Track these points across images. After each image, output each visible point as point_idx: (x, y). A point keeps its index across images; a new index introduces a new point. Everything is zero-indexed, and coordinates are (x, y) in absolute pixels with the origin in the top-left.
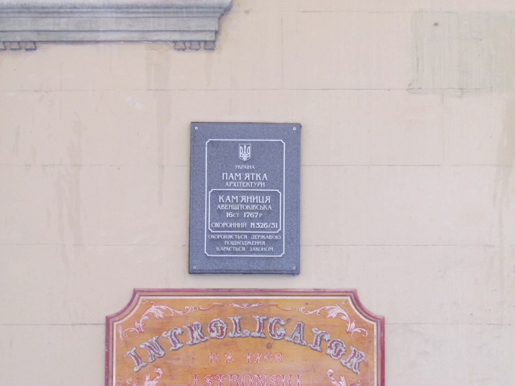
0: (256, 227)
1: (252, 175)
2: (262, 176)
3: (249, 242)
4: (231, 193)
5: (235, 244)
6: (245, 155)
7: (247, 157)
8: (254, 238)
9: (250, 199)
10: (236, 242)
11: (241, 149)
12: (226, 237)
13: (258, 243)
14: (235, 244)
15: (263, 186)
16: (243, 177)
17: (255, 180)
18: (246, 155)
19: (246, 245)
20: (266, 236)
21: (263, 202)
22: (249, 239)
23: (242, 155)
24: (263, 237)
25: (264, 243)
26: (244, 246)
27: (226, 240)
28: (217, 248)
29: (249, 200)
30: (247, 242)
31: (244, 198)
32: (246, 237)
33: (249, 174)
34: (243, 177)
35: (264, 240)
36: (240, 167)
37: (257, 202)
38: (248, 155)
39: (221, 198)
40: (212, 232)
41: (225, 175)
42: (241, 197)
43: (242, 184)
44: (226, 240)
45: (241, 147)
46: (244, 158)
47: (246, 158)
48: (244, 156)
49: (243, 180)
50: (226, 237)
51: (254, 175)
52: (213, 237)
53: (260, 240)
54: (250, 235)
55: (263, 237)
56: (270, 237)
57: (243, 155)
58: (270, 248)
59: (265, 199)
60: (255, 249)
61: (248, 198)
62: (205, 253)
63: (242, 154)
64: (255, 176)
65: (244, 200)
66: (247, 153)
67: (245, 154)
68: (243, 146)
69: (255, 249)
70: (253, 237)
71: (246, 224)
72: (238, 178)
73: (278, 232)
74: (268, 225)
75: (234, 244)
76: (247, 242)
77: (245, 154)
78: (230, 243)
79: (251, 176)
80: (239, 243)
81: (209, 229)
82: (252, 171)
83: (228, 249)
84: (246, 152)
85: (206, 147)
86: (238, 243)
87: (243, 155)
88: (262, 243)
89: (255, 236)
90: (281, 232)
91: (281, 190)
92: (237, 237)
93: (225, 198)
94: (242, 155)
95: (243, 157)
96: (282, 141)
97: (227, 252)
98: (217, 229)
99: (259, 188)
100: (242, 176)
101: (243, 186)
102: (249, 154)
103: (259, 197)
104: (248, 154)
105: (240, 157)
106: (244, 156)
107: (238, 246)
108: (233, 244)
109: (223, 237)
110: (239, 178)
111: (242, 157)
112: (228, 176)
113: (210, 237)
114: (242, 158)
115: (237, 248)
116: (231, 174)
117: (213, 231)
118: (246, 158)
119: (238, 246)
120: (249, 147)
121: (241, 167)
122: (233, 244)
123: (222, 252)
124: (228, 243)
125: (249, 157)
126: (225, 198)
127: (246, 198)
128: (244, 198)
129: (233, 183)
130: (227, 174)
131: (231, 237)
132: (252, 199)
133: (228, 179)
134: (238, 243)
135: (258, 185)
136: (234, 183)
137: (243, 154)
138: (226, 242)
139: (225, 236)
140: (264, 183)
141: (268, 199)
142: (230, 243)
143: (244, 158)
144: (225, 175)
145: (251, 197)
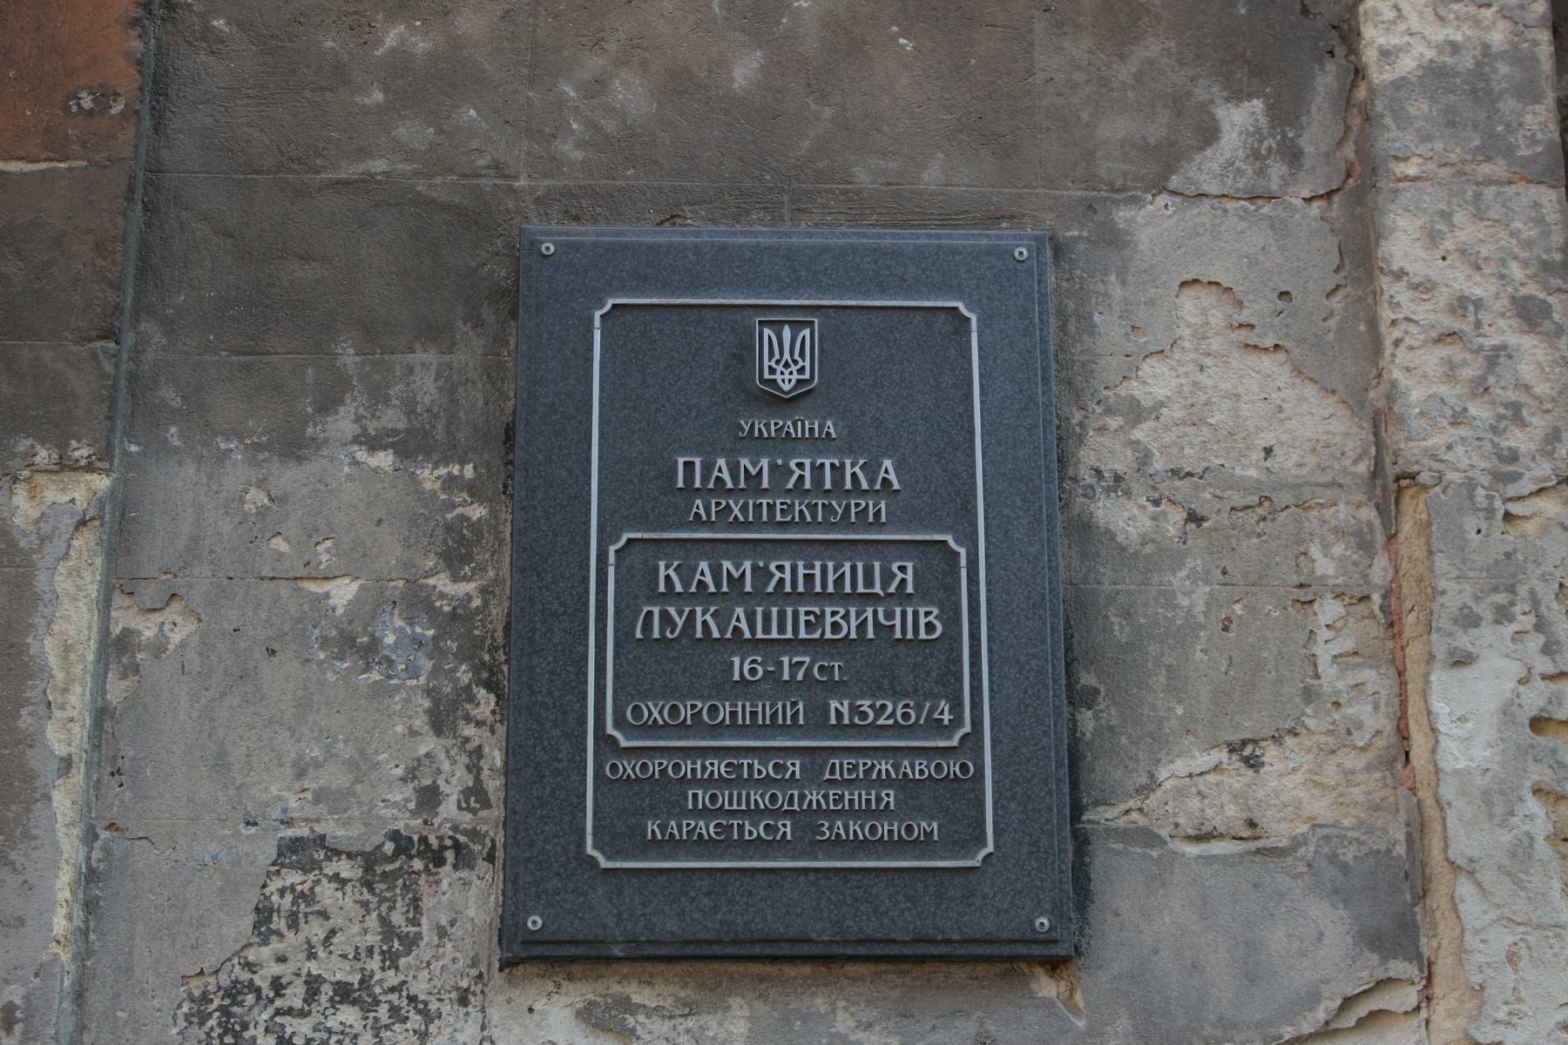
0: (856, 721)
1: (822, 465)
2: (871, 469)
3: (814, 796)
6: (787, 372)
7: (795, 377)
8: (838, 776)
9: (813, 575)
10: (748, 796)
12: (694, 770)
13: (859, 796)
14: (739, 804)
15: (877, 514)
16: (780, 472)
18: (794, 368)
20: (896, 767)
21: (877, 589)
22: (812, 776)
24: (884, 766)
25: (890, 797)
26: (790, 814)
27: (694, 782)
28: (652, 826)
29: (809, 578)
30: (802, 797)
31: (780, 568)
32: (795, 767)
33: (807, 462)
34: (780, 472)
35: (888, 782)
36: (764, 425)
37: (848, 589)
38: (801, 371)
41: (689, 466)
42: (766, 567)
43: (771, 507)
44: (694, 782)
45: (767, 332)
47: (790, 381)
48: (782, 373)
49: (777, 488)
50: (694, 770)
51: (832, 465)
52: (628, 768)
53: (868, 782)
56: (917, 769)
58: (923, 824)
61: (801, 571)
63: (774, 365)
64: (838, 470)
65: (781, 580)
66: (795, 362)
68: (777, 326)
70: (832, 772)
71: (800, 706)
74: (919, 708)
75: (735, 807)
76: (802, 797)
77: (787, 365)
78: (713, 798)
79: (818, 470)
80: (762, 796)
81: (610, 730)
82: (821, 443)
85: (597, 335)
86: (759, 798)
87: (780, 368)
88: (879, 800)
92: (750, 766)
93: (686, 573)
94: (772, 371)
95: (778, 377)
96: (960, 306)
97: (702, 846)
99: (850, 526)
100: (773, 467)
101: (779, 518)
102: (807, 364)
103: (860, 566)
104: (799, 366)
105: (763, 381)
106: (782, 373)
107: (754, 814)
108: (731, 803)
109: (677, 767)
110: (760, 482)
112: (708, 468)
113: (614, 768)
114: (775, 380)
115: (750, 825)
116: (721, 462)
117: (627, 738)
118: (793, 382)
119: (754, 814)
120: (807, 332)
121: (767, 426)
122: (731, 803)
123: (671, 846)
125: (807, 376)
127: (794, 569)
130: (697, 461)
131: (718, 767)
132: (828, 573)
133: (705, 478)
134: (759, 798)
135: (853, 510)
136: (731, 502)
137: (778, 362)
138: (694, 796)
139: (689, 766)
140: (883, 505)
141: (907, 573)
142: (713, 798)
144: (689, 466)
145: (818, 564)
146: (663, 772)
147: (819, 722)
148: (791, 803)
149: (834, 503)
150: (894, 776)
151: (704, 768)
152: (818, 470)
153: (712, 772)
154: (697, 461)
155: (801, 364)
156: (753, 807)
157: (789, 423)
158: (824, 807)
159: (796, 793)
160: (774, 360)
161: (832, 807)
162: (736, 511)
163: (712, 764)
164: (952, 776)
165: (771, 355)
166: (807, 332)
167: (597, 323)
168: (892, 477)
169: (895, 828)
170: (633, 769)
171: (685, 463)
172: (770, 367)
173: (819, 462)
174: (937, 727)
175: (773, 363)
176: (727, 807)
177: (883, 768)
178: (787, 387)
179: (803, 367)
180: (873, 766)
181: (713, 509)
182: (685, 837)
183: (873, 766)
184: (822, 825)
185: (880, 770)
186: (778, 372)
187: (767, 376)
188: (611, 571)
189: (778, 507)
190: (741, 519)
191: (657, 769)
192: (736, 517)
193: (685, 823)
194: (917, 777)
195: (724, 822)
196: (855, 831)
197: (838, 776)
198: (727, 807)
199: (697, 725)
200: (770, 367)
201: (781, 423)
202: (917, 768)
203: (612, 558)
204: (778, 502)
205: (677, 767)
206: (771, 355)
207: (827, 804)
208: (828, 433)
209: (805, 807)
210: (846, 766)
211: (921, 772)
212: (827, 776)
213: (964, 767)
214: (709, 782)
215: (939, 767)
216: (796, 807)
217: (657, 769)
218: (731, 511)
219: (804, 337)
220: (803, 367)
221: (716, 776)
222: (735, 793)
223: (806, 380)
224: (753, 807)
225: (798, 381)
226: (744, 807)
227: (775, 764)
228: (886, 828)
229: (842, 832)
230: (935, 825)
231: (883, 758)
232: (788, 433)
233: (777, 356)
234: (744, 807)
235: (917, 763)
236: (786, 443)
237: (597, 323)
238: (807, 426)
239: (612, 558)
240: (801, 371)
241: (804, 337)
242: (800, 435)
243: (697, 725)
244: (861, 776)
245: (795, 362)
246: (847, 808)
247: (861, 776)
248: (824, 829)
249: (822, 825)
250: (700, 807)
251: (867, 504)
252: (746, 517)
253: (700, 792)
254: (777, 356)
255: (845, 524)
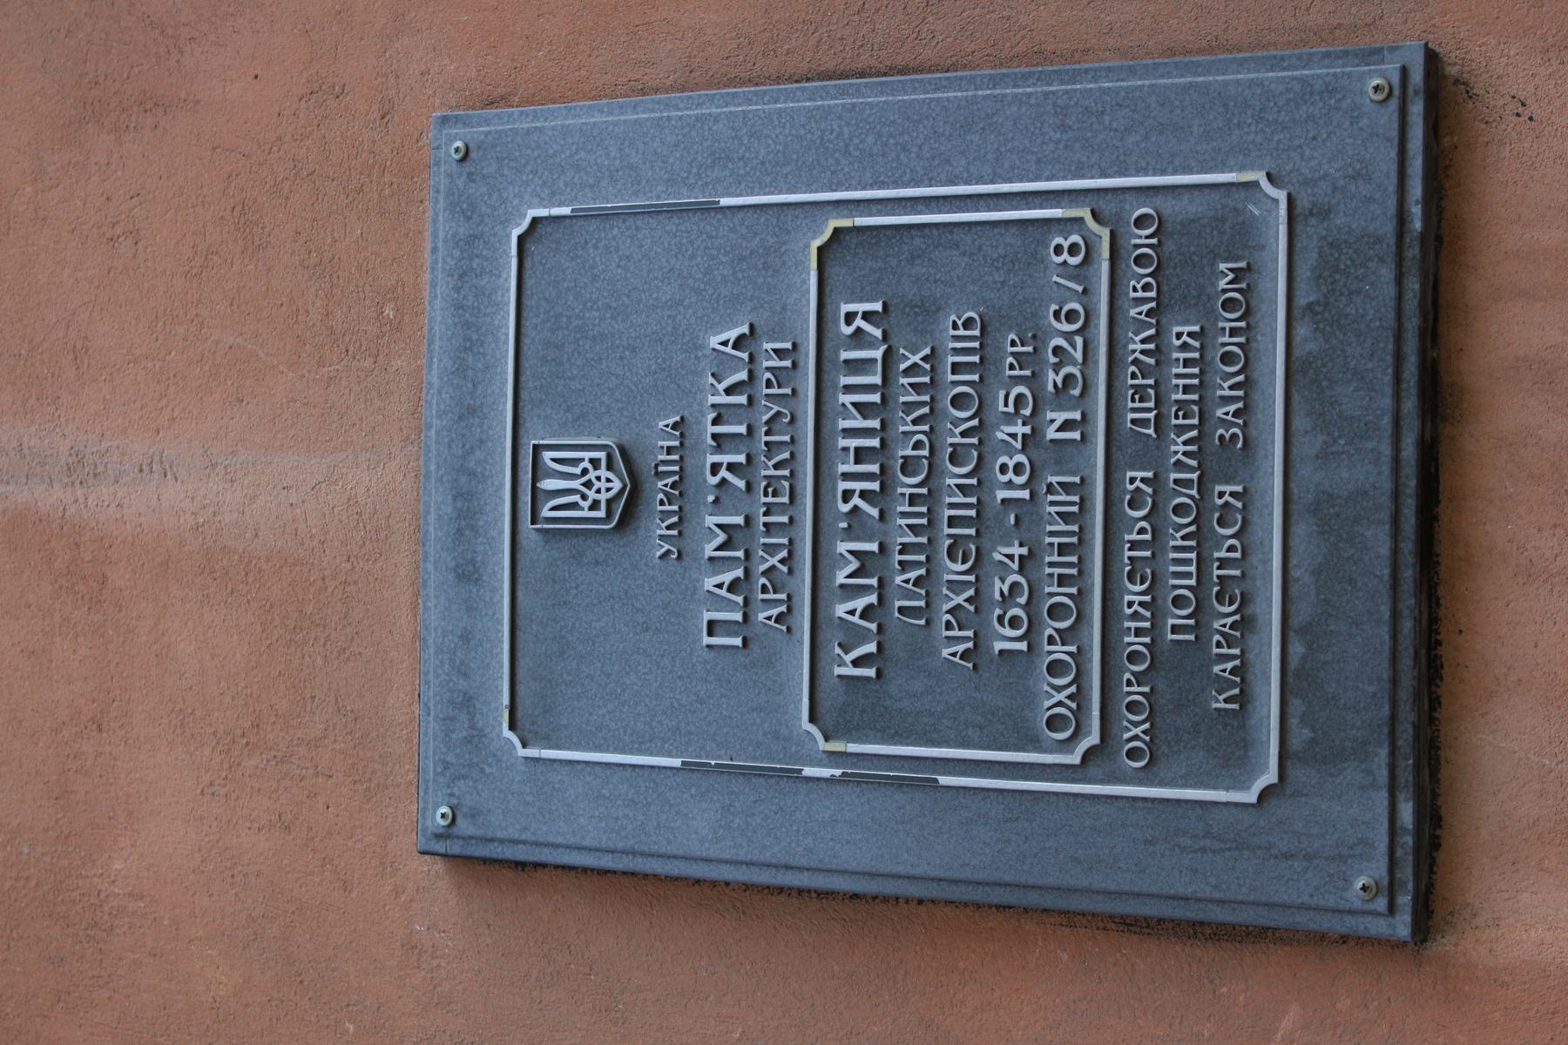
5: (1187, 562)
6: (597, 485)
7: (603, 472)
8: (1151, 415)
10: (1177, 549)
11: (553, 509)
14: (1187, 562)
18: (592, 475)
19: (1195, 476)
22: (1151, 453)
23: (595, 506)
40: (1093, 739)
41: (712, 627)
45: (546, 512)
46: (608, 490)
48: (598, 491)
51: (715, 422)
57: (592, 495)
60: (1227, 400)
62: (1251, 797)
66: (585, 472)
67: (588, 484)
69: (1227, 400)
73: (1105, 234)
75: (1193, 569)
77: (588, 484)
78: (1178, 602)
81: (1075, 759)
83: (1229, 620)
84: (572, 477)
89: (1134, 410)
94: (595, 506)
95: (603, 497)
102: (587, 455)
104: (590, 467)
106: (598, 491)
108: (1188, 575)
109: (1134, 657)
111: (603, 506)
114: (609, 502)
118: (611, 475)
120: (547, 455)
122: (1188, 575)
124: (1179, 616)
125: (602, 455)
129: (764, 573)
131: (1134, 593)
137: (584, 497)
139: (1132, 639)
140: (768, 346)
142: (1178, 602)
143: (608, 490)
146: (1140, 678)
148: (1186, 483)
149: (765, 418)
150: (1152, 332)
151: (1135, 616)
153: (1141, 604)
154: (708, 616)
155: (586, 464)
156: (1193, 543)
157: (660, 484)
158: (1194, 433)
159: (1173, 476)
160: (582, 503)
161: (1195, 421)
162: (774, 561)
163: (1130, 604)
164: (1154, 241)
165: (573, 506)
166: (547, 455)
167: (532, 752)
168: (732, 335)
169: (1228, 325)
170: (1136, 724)
171: (710, 634)
172: (591, 508)
173: (710, 442)
175: (586, 504)
176: (1193, 582)
177: (1140, 347)
178: (617, 485)
179: (592, 461)
180: (1136, 362)
181: (771, 596)
182: (1236, 651)
183: (1136, 362)
184: (1221, 437)
185: (1143, 352)
186: (597, 496)
187: (601, 514)
188: (853, 748)
189: (770, 499)
190: (784, 554)
191: (1135, 689)
192: (782, 561)
193: (1216, 651)
194: (1153, 294)
195: (1216, 589)
196: (1231, 388)
197: (1151, 415)
198: (1193, 582)
200: (591, 508)
201: (661, 496)
202: (1140, 294)
203: (836, 746)
204: (764, 500)
205: (1134, 657)
206: (573, 506)
207: (1191, 427)
208: (675, 426)
209: (1194, 463)
210: (1137, 405)
211: (1146, 288)
212: (1151, 431)
213: (1141, 222)
215: (1139, 261)
216: (1195, 476)
217: (1135, 689)
218: (773, 567)
219: (554, 460)
220: (592, 461)
221: (1147, 598)
222: (1173, 569)
223: (610, 458)
224: (1193, 543)
225: (609, 467)
226: (1193, 556)
227: (1132, 505)
228: (1226, 339)
229: (1232, 408)
230: (1223, 266)
231: (1126, 346)
232: (673, 486)
233: (576, 498)
234: (1193, 556)
235: (1132, 295)
237: (532, 752)
238: (663, 457)
239: (836, 746)
240: (595, 463)
241: (554, 460)
242: (676, 468)
244: (1151, 382)
245: (585, 472)
246: (1195, 397)
247: (1151, 382)
248: (1227, 436)
249: (1221, 437)
250: (1192, 622)
251: (768, 369)
252: (779, 546)
253: (1171, 621)
254: (576, 498)
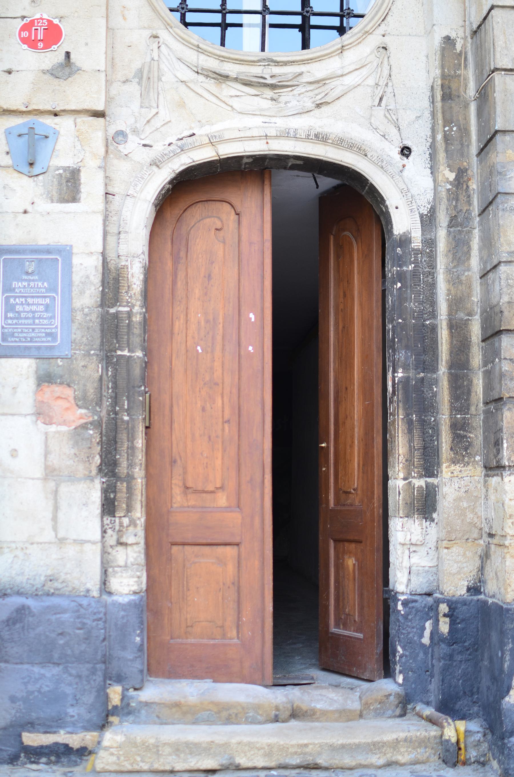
2: (43, 284)
4: (19, 297)
17: (38, 288)
24: (43, 330)
32: (31, 330)
39: (12, 300)
44: (16, 332)
52: (6, 330)
53: (41, 332)
54: (33, 329)
55: (43, 330)
59: (45, 301)
64: (38, 284)
72: (25, 286)
79: (35, 284)
81: (3, 324)
90: (56, 327)
91: (57, 295)
98: (10, 324)
123: (12, 342)
126: (15, 300)
128: (30, 300)
147: (34, 323)
152: (35, 284)
174: (51, 324)
199: (16, 324)
214: (18, 332)
236: (30, 280)
243: (16, 324)
255: (38, 293)
